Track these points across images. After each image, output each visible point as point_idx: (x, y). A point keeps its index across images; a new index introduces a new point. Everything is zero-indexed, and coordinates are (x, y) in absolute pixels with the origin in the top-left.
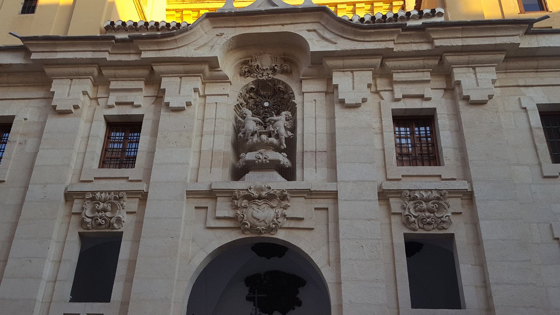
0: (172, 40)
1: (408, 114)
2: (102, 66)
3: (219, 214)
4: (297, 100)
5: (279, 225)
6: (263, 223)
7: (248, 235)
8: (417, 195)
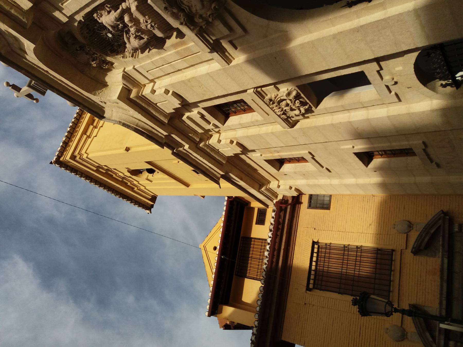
0: (139, 127)
2: (195, 143)
3: (226, 31)
4: (79, 17)
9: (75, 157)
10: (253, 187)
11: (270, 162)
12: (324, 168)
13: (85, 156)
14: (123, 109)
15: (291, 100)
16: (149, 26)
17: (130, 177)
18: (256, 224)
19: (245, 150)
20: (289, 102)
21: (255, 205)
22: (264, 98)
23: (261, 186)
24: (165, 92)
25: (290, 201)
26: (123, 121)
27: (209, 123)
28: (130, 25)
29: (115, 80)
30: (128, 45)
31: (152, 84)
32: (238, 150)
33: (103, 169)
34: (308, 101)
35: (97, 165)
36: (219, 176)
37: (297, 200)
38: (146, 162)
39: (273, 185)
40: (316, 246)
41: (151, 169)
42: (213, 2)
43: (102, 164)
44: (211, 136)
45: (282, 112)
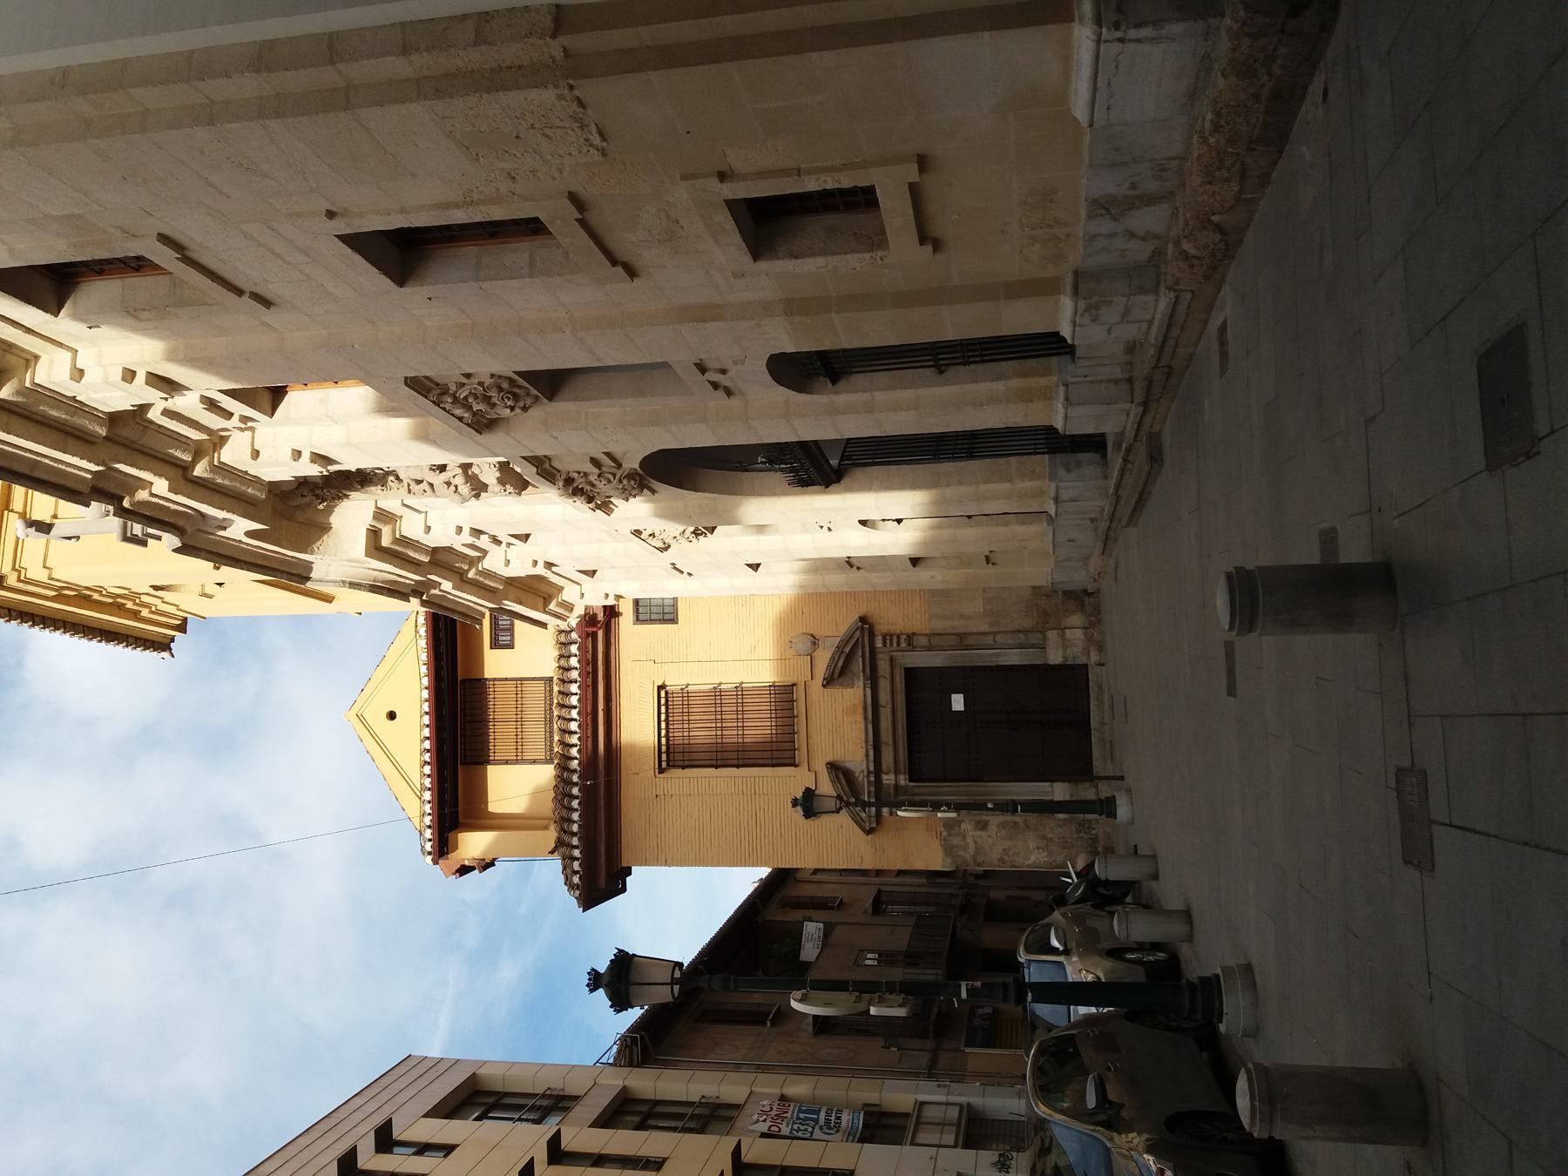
23: (547, 600)
25: (601, 617)
37: (611, 612)
40: (663, 694)
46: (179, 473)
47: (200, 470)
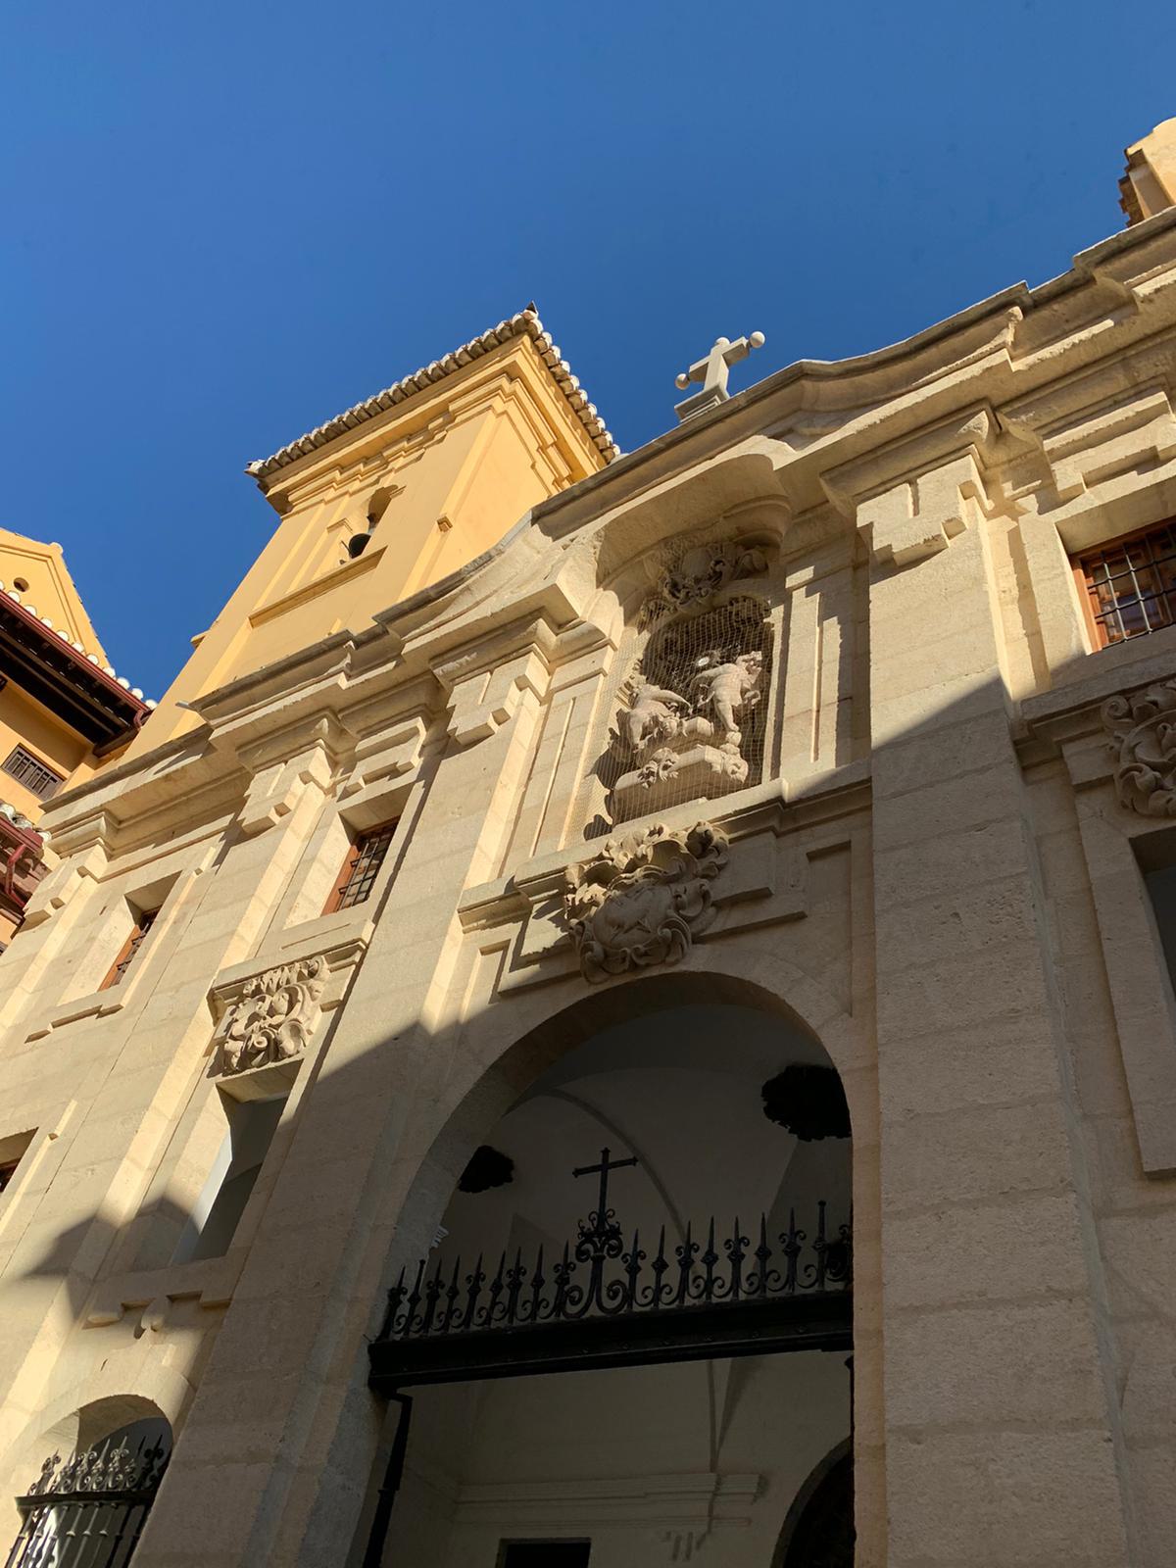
1: (1124, 526)
2: (341, 711)
5: (690, 930)
6: (636, 934)
7: (603, 985)
8: (1152, 697)
9: (511, 380)
10: (124, 797)
11: (166, 885)
12: (50, 1028)
13: (498, 403)
14: (527, 582)
15: (278, 1026)
16: (654, 767)
17: (377, 481)
18: (20, 746)
19: (238, 835)
20: (276, 1020)
21: (85, 774)
22: (331, 961)
23: (117, 824)
24: (502, 710)
25: (17, 879)
26: (498, 560)
27: (370, 779)
28: (686, 724)
29: (602, 611)
30: (655, 689)
31: (543, 693)
32: (249, 816)
33: (441, 428)
34: (248, 1072)
35: (457, 421)
36: (213, 723)
38: (385, 549)
39: (96, 859)
41: (360, 553)
42: (605, 952)
43: (453, 435)
44: (334, 764)
45: (263, 988)
46: (996, 401)
47: (982, 420)
